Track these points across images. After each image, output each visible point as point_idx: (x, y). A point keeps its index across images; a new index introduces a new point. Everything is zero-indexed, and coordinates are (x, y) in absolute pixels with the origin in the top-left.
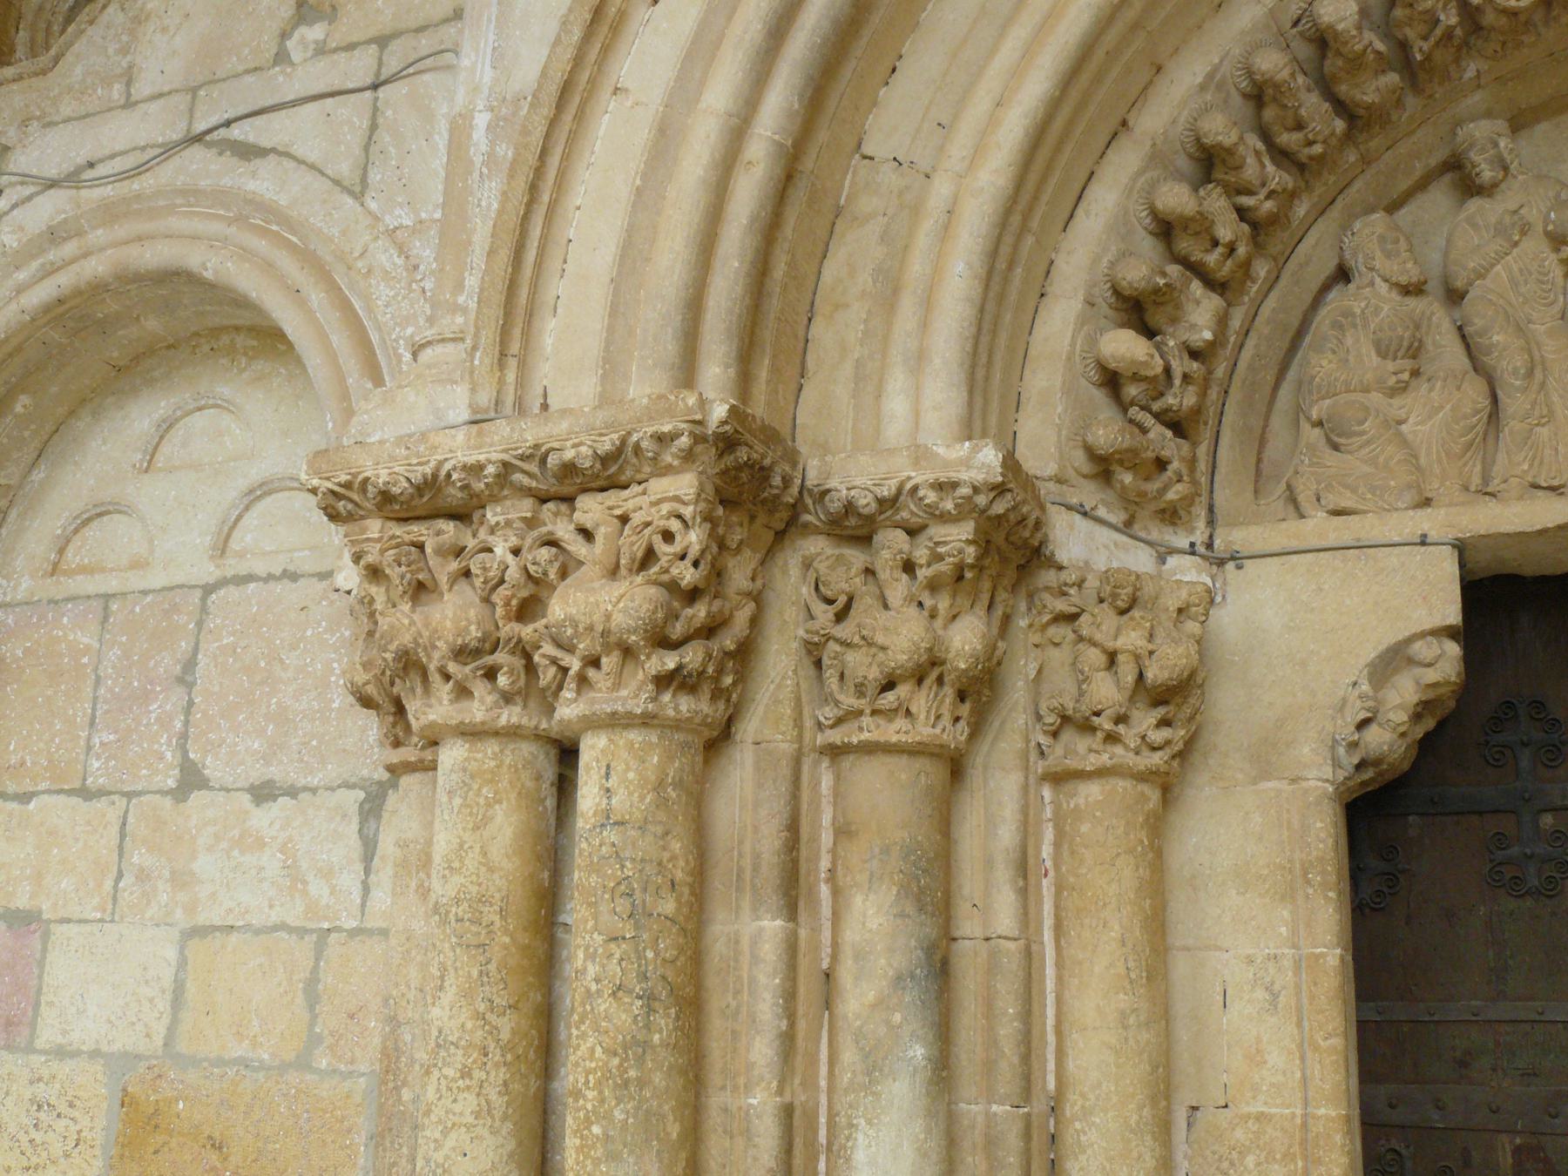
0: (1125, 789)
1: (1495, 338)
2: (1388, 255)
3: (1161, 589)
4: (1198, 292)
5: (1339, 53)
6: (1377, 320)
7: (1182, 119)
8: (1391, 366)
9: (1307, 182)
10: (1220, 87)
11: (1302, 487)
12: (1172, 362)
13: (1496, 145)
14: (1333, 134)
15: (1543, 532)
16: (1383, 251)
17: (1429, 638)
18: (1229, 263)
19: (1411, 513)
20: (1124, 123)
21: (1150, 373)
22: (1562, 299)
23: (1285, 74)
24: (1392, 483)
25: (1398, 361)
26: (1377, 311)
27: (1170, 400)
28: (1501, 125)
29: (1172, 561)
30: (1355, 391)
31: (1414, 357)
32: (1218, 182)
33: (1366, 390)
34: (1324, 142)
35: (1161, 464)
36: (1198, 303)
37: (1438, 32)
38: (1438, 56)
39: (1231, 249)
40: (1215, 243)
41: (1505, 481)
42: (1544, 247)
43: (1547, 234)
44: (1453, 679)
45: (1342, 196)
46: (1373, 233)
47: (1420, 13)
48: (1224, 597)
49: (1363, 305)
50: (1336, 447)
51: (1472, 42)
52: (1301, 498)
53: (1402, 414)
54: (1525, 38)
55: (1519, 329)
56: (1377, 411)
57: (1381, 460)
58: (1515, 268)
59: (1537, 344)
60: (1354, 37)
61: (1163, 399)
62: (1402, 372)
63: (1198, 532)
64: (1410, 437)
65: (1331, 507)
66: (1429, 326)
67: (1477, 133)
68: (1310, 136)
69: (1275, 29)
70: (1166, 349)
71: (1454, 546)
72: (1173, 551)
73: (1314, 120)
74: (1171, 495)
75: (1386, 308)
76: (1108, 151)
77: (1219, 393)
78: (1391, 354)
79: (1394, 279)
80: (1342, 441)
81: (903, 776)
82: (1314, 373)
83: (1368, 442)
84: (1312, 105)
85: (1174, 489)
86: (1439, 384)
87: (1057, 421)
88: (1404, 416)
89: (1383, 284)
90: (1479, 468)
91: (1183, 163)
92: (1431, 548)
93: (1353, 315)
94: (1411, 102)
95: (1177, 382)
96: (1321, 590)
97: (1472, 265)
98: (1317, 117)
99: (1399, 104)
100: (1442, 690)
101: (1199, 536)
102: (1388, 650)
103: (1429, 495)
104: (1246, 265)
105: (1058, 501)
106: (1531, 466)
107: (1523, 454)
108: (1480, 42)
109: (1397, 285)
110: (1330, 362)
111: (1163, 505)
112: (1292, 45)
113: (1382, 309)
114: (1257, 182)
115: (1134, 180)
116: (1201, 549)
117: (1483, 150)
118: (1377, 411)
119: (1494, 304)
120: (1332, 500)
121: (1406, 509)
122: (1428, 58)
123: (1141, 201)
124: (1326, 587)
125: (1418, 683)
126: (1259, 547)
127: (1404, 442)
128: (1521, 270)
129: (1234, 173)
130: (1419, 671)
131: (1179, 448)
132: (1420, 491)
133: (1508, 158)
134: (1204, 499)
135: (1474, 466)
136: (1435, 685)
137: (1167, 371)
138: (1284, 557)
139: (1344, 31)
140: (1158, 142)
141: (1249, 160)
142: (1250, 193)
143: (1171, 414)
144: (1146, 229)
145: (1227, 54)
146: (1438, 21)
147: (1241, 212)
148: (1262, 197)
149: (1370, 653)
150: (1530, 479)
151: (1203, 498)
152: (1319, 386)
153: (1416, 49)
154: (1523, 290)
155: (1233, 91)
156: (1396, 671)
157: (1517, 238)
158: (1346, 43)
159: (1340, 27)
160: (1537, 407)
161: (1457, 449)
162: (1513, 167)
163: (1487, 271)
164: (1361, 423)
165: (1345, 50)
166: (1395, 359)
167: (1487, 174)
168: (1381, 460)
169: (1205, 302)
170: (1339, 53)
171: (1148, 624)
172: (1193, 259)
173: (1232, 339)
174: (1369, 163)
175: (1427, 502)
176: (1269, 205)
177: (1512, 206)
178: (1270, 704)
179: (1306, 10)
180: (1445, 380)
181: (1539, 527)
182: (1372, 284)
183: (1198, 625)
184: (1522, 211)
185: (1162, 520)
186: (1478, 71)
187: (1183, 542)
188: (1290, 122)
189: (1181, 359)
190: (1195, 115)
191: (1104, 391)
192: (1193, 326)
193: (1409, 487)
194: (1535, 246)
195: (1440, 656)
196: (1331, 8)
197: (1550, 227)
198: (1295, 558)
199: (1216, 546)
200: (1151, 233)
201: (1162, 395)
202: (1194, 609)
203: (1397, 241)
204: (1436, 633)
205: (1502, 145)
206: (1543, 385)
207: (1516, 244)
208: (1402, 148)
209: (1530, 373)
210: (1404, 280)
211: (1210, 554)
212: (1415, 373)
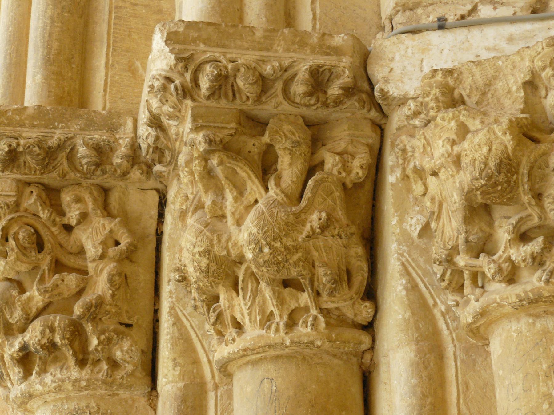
0: (519, 332)
3: (498, 70)
81: (249, 389)
171: (453, 124)
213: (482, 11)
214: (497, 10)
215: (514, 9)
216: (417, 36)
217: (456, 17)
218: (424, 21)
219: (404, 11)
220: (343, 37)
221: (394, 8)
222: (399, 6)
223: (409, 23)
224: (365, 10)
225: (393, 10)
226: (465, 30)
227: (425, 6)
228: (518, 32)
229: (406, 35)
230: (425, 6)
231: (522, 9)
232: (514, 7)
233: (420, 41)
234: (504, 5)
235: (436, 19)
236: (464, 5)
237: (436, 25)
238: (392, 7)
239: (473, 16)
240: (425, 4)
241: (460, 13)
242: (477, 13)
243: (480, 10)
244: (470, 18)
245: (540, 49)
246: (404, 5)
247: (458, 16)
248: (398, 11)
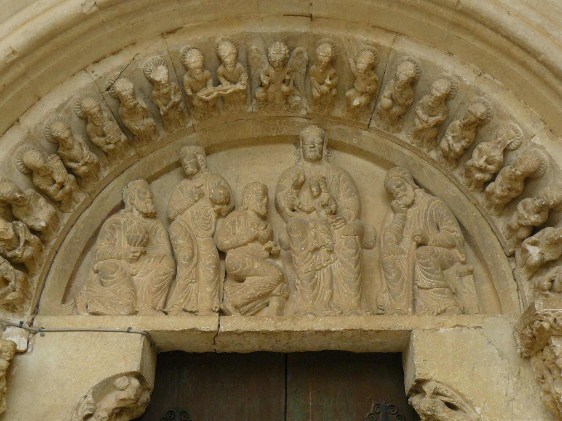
1: (179, 241)
2: (140, 198)
4: (42, 204)
5: (124, 106)
6: (130, 227)
7: (45, 123)
8: (133, 249)
9: (109, 161)
10: (67, 111)
11: (80, 300)
12: (20, 234)
13: (196, 157)
14: (119, 141)
15: (183, 331)
16: (139, 197)
17: (124, 377)
18: (61, 192)
19: (126, 317)
20: (18, 121)
21: (6, 238)
22: (213, 228)
23: (95, 110)
24: (121, 302)
25: (136, 247)
26: (131, 222)
27: (17, 252)
28: (200, 149)
29: (9, 330)
30: (114, 258)
31: (145, 246)
32: (58, 154)
33: (120, 258)
34: (115, 144)
35: (7, 282)
36: (41, 208)
37: (170, 104)
38: (172, 114)
39: (62, 186)
40: (54, 182)
41: (173, 307)
42: (209, 204)
43: (210, 199)
44: (132, 397)
45: (127, 170)
46: (136, 188)
47: (163, 94)
48: (32, 350)
49: (125, 220)
50: (102, 284)
51: (191, 111)
52: (78, 305)
53: (134, 271)
54: (213, 113)
55: (190, 238)
56: (122, 269)
57: (118, 291)
58: (195, 211)
59: (197, 246)
60: (130, 99)
61: (14, 251)
62: (137, 252)
63: (26, 317)
64: (136, 282)
65: (92, 311)
66: (155, 233)
67: (188, 151)
68: (108, 140)
69: (97, 90)
70: (18, 227)
71: (143, 334)
72: (10, 325)
73: (109, 133)
74: (9, 297)
75: (135, 223)
76: (7, 132)
77: (51, 252)
78: (133, 243)
79: (141, 210)
80: (104, 280)
82: (98, 248)
83: (114, 283)
84: (111, 127)
85: (11, 295)
86: (153, 260)
88: (135, 272)
89: (136, 211)
90: (163, 299)
91: (45, 144)
92: (132, 334)
93: (120, 224)
94: (163, 133)
95: (22, 244)
96: (78, 349)
97: (177, 208)
98: (111, 132)
99: (155, 131)
100: (128, 403)
101: (26, 319)
102: (104, 381)
103: (137, 310)
104: (70, 194)
106: (184, 301)
107: (182, 295)
108: (194, 112)
109: (141, 212)
110: (106, 244)
111: (6, 302)
112: (105, 98)
113: (134, 223)
114: (80, 158)
115: (16, 147)
116: (27, 326)
117: (189, 159)
118: (122, 269)
119: (182, 227)
120: (92, 308)
121: (125, 315)
122: (166, 114)
123: (18, 157)
124: (81, 349)
125: (116, 398)
126: (54, 327)
127: (132, 284)
128: (197, 213)
129: (67, 151)
130: (117, 392)
131: (16, 275)
132: (133, 307)
133: (201, 163)
134: (33, 301)
135: (161, 298)
136: (124, 400)
137: (18, 238)
138: (64, 333)
139: (125, 96)
140: (32, 131)
141: (75, 146)
142: (77, 162)
143: (17, 259)
144: (20, 170)
145: (72, 97)
146: (171, 99)
147: (70, 170)
148: (80, 164)
149: (95, 382)
150: (183, 307)
151: (32, 301)
152: (99, 254)
153: (161, 110)
154: (196, 222)
155: (74, 115)
156: (109, 392)
157: (197, 199)
158: (126, 101)
159: (124, 94)
160: (192, 274)
161: (153, 289)
162: (203, 168)
163: (183, 212)
164: (113, 273)
165: (126, 104)
166: (135, 246)
167: (190, 169)
168: (118, 291)
169: (45, 208)
170: (124, 106)
172: (41, 188)
173: (62, 228)
174: (142, 157)
175: (135, 313)
176: (84, 169)
177: (198, 185)
178: (43, 404)
179: (112, 84)
180: (155, 258)
181: (181, 329)
182: (131, 211)
183: (5, 362)
184: (202, 188)
185: (8, 310)
186: (193, 124)
187: (17, 321)
188: (100, 133)
189: (25, 233)
190: (52, 122)
192: (37, 219)
193: (128, 305)
194: (204, 203)
195: (128, 386)
196: (121, 85)
197: (211, 196)
198: (69, 333)
199: (34, 324)
200: (23, 173)
201: (15, 249)
202: (4, 354)
203: (145, 193)
204: (129, 374)
205: (199, 157)
206: (196, 265)
207: (196, 201)
208: (158, 153)
209: (191, 258)
210: (145, 211)
211: (30, 328)
212: (144, 253)
245: (8, 344)
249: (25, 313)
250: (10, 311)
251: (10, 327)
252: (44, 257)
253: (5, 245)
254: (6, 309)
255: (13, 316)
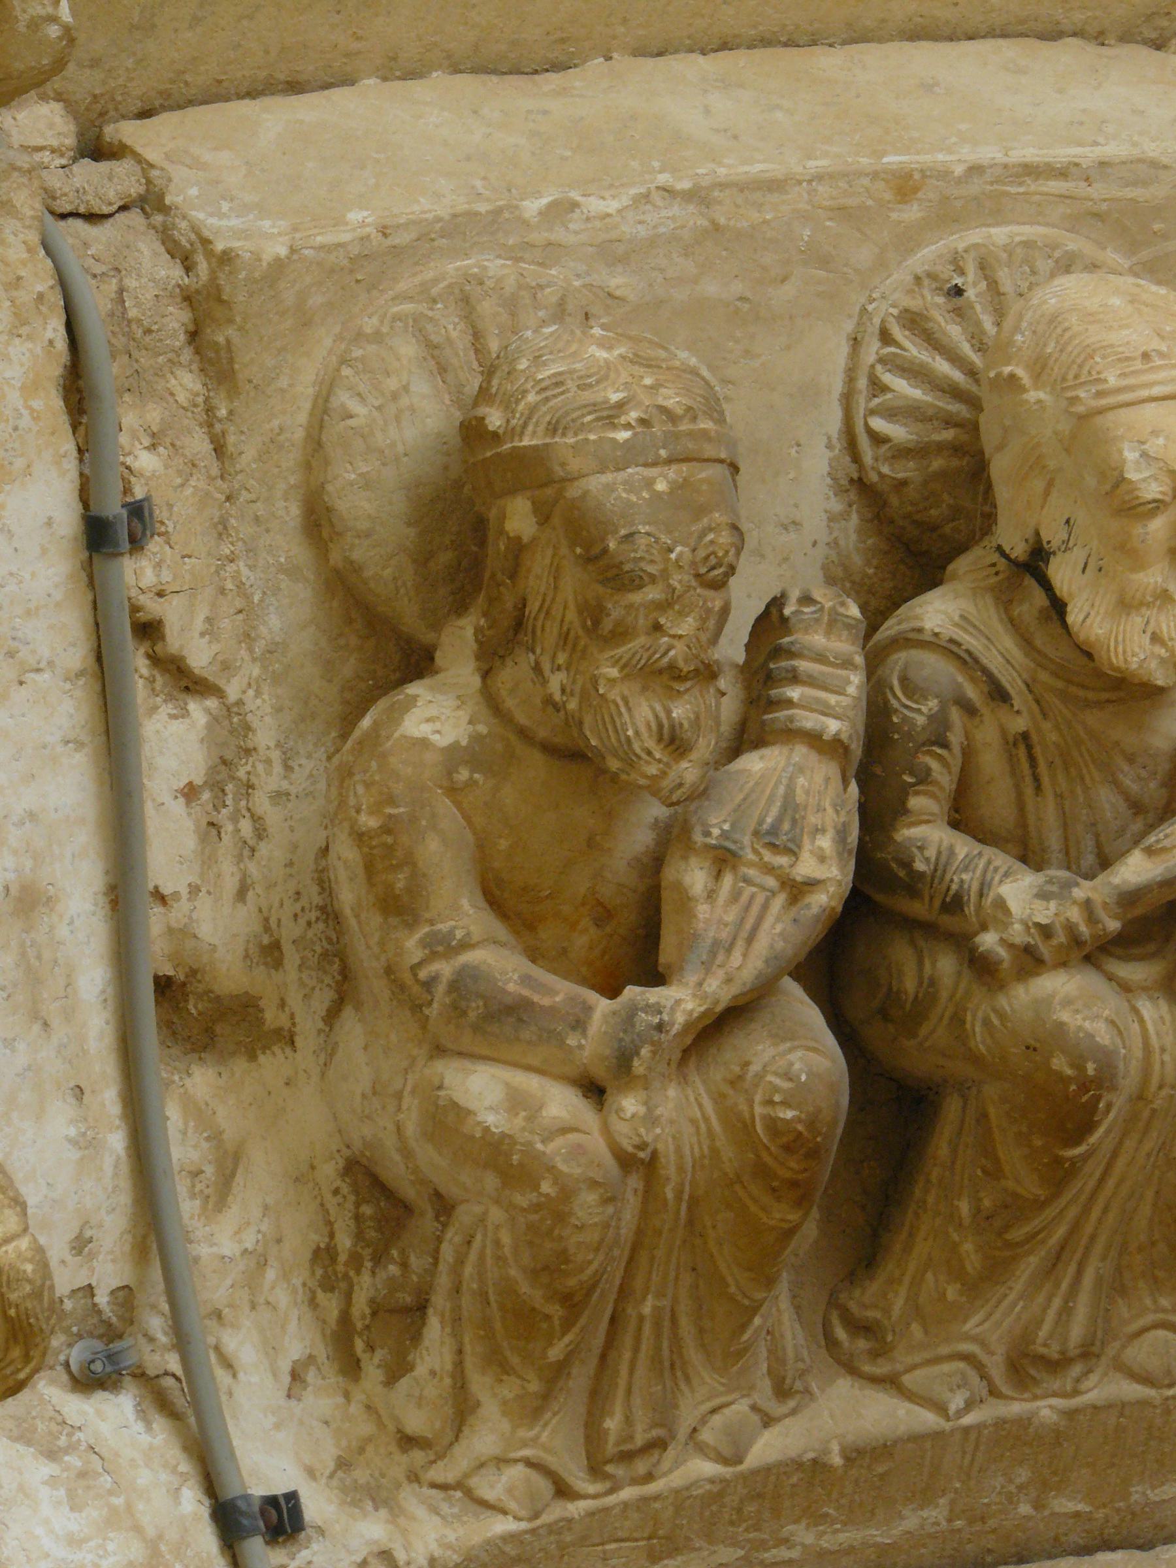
61: (1001, 860)
87: (532, 207)
105: (96, 334)
191: (850, 531)
213: (177, 726)
214: (178, 807)
215: (184, 892)
216: (52, 402)
217: (144, 600)
218: (129, 419)
219: (188, 298)
220: (53, 19)
221: (206, 242)
222: (212, 272)
223: (120, 342)
224: (196, 20)
225: (195, 229)
226: (77, 656)
227: (210, 410)
228: (63, 932)
229: (61, 344)
230: (210, 410)
231: (181, 934)
232: (194, 890)
233: (26, 421)
234: (203, 839)
235: (139, 493)
236: (211, 630)
237: (113, 507)
238: (210, 222)
239: (151, 681)
240: (223, 412)
241: (171, 613)
242: (170, 698)
243: (185, 714)
244: (141, 664)
246: (220, 301)
247: (153, 607)
248: (188, 267)
249: (411, 1499)
250: (331, 1305)
251: (160, 1423)
252: (1140, 1353)
253: (999, 694)
254: (324, 1255)
255: (296, 1376)
